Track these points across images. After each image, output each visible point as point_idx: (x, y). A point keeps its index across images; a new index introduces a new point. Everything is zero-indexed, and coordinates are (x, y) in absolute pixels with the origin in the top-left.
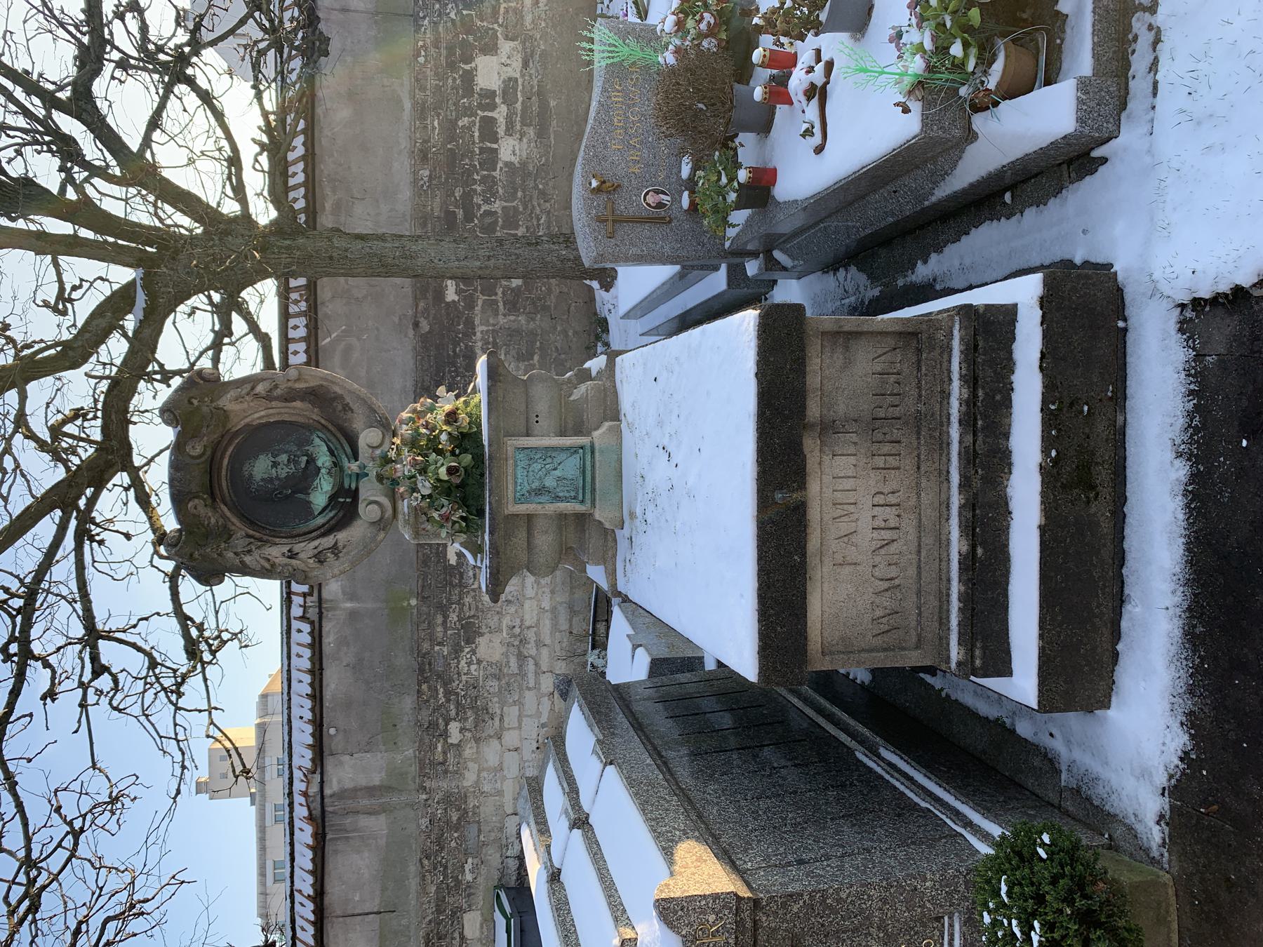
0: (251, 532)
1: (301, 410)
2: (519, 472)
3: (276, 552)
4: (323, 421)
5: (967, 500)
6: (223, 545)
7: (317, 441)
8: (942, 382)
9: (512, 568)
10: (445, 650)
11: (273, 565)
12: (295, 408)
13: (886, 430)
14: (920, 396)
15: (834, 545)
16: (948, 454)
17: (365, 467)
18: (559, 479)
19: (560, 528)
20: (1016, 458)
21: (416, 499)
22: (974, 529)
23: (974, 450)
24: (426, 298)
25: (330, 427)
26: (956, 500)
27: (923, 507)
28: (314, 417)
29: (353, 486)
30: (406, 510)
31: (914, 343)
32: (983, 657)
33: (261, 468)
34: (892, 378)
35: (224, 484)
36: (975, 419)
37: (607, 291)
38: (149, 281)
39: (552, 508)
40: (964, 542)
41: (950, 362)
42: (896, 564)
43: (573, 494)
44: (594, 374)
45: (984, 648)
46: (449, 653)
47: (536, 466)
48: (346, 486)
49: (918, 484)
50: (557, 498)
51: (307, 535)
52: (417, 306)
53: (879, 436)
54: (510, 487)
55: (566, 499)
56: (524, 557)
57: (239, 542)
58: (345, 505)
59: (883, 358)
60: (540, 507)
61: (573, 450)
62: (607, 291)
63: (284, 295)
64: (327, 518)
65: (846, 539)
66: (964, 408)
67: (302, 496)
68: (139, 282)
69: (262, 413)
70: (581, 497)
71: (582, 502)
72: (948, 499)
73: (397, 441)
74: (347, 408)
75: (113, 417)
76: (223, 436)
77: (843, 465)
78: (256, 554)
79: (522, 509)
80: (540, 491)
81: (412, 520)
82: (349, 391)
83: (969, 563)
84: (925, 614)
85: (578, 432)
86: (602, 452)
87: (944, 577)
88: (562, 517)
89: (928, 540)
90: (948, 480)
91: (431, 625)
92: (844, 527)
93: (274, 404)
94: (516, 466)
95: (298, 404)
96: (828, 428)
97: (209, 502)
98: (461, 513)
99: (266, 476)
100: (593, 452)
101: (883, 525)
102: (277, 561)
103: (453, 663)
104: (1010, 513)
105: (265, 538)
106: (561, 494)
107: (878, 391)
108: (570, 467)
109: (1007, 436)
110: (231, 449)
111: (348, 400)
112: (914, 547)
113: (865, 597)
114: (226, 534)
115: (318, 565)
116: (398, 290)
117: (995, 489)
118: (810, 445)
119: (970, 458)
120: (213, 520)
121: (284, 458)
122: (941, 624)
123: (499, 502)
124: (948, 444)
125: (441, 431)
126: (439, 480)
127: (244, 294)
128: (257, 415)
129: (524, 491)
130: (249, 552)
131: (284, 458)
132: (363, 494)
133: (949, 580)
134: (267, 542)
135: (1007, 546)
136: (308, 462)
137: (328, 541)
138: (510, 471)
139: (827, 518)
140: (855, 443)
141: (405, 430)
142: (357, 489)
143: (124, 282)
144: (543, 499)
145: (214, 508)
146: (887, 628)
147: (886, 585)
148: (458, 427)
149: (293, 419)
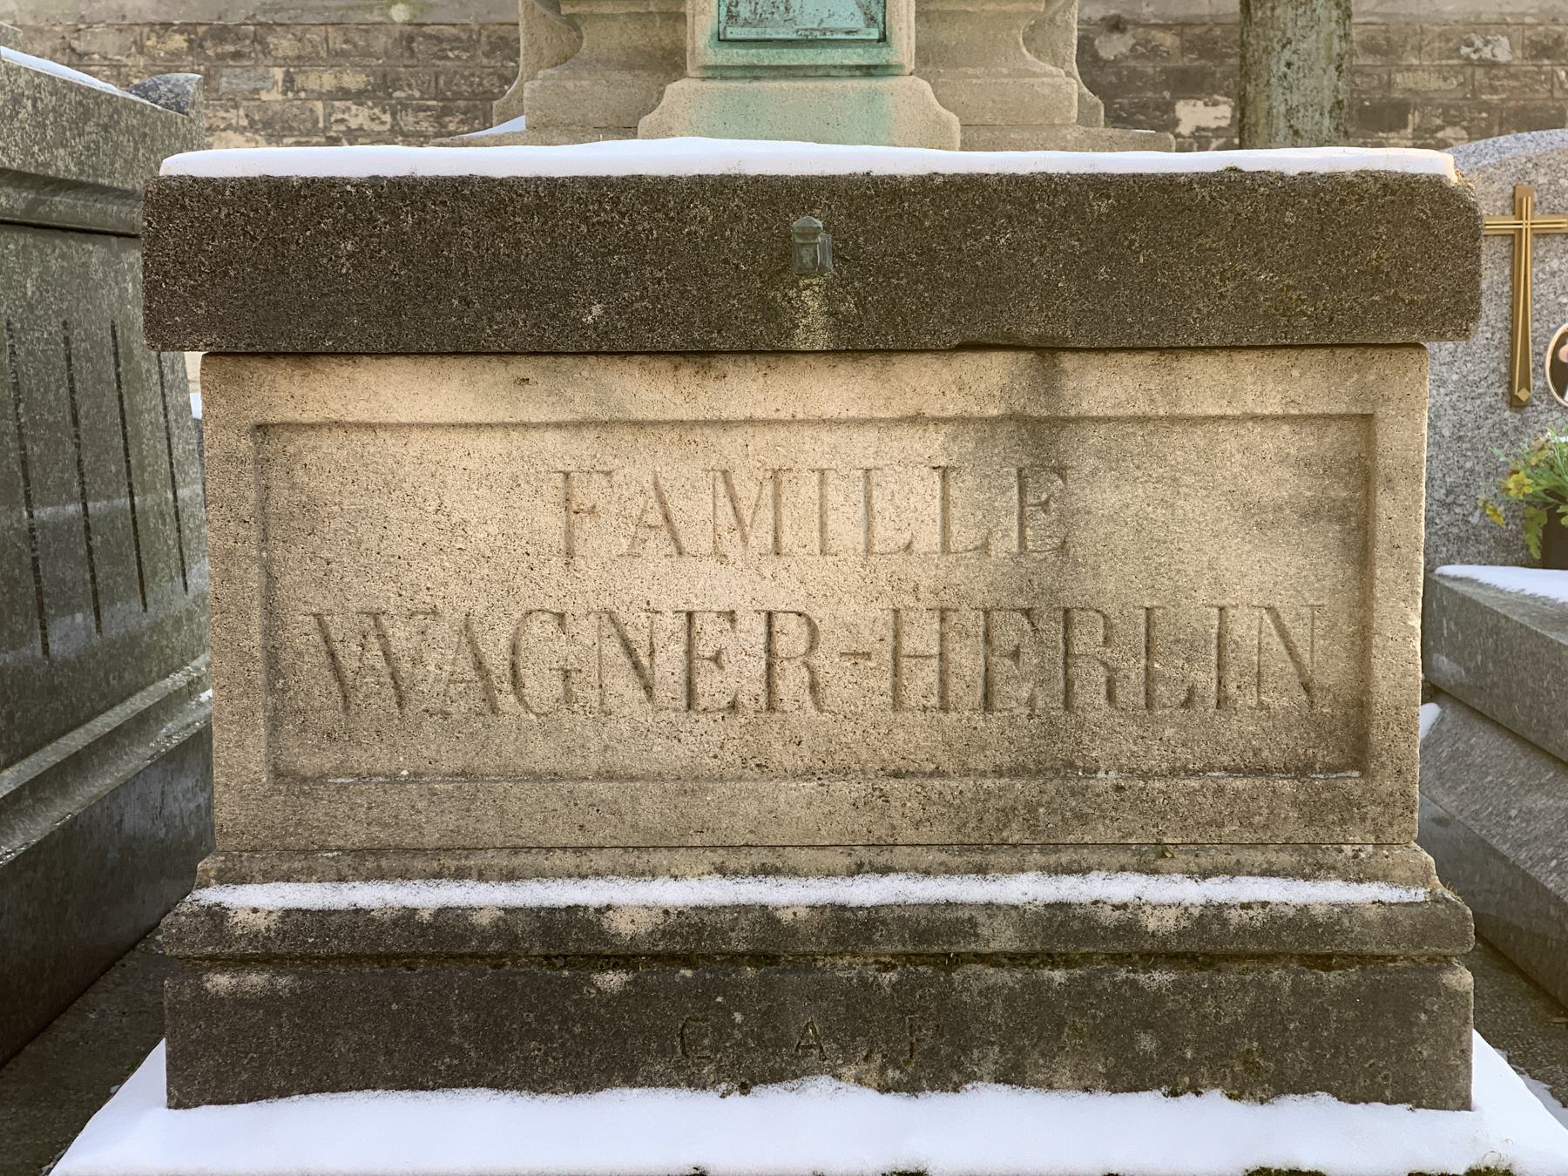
5: (791, 931)
8: (1198, 848)
10: (272, 96)
13: (1030, 659)
14: (1146, 776)
15: (638, 467)
16: (950, 871)
20: (934, 1107)
22: (687, 960)
23: (959, 960)
24: (1184, 51)
26: (790, 895)
27: (766, 787)
31: (1322, 756)
32: (239, 1001)
34: (1205, 678)
36: (1068, 963)
40: (645, 924)
41: (1268, 872)
42: (568, 697)
45: (269, 1002)
46: (263, 106)
49: (844, 772)
52: (1165, 27)
53: (1007, 636)
59: (1276, 643)
65: (655, 517)
66: (1108, 917)
70: (734, 32)
72: (794, 872)
77: (912, 504)
83: (573, 941)
84: (393, 797)
86: (872, 98)
87: (517, 861)
89: (651, 808)
90: (857, 870)
91: (336, 58)
92: (698, 509)
96: (1038, 444)
100: (868, 71)
101: (705, 649)
103: (238, 117)
104: (745, 1089)
107: (1162, 629)
109: (1012, 1075)
112: (622, 759)
113: (455, 588)
117: (830, 1034)
118: (989, 381)
119: (936, 940)
122: (360, 853)
124: (981, 870)
133: (511, 876)
135: (630, 1081)
139: (730, 445)
140: (984, 548)
146: (349, 664)
147: (497, 661)
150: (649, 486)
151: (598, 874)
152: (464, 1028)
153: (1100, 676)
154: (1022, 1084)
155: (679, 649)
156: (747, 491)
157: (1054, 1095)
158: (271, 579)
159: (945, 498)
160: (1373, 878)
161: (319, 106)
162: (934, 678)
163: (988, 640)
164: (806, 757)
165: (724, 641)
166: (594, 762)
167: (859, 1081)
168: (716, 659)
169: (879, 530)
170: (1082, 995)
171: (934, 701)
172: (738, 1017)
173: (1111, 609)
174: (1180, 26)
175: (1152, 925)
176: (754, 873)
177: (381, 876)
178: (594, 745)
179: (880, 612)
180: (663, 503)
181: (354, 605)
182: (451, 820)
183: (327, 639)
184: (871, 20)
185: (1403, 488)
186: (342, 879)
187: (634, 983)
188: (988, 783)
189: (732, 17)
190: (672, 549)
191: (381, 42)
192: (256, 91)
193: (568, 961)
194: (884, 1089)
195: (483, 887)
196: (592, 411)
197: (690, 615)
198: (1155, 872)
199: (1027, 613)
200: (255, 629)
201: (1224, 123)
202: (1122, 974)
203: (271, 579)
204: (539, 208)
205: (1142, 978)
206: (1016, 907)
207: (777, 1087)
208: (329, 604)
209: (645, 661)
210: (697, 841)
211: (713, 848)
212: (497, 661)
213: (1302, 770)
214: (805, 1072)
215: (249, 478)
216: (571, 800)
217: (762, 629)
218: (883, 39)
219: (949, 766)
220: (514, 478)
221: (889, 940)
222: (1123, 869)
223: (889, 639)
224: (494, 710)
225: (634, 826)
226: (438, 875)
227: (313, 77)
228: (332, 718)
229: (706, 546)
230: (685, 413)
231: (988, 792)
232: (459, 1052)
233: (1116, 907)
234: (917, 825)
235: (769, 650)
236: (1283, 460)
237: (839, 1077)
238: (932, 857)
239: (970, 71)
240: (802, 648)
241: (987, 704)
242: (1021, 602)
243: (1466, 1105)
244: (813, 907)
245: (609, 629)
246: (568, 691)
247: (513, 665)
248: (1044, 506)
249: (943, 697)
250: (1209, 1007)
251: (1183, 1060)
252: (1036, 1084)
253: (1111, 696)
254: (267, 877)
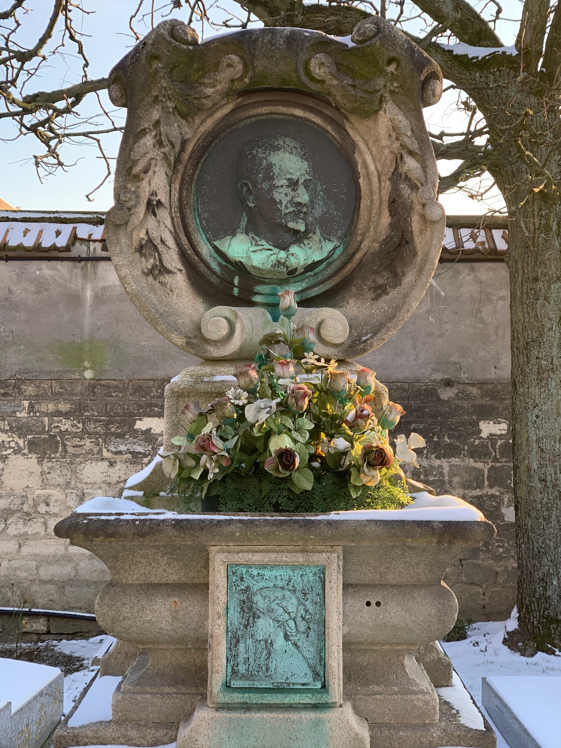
0: (190, 147)
1: (376, 224)
2: (282, 573)
3: (157, 182)
4: (358, 256)
6: (170, 104)
7: (328, 247)
9: (115, 558)
11: (137, 178)
12: (379, 215)
17: (289, 316)
18: (269, 644)
19: (182, 641)
21: (238, 398)
24: (483, 396)
25: (350, 267)
28: (365, 244)
29: (257, 299)
30: (218, 378)
33: (289, 163)
35: (260, 110)
37: (505, 642)
38: (501, 61)
39: (218, 630)
43: (242, 669)
44: (445, 693)
46: (18, 420)
47: (292, 604)
48: (258, 288)
50: (234, 640)
51: (183, 229)
52: (473, 385)
54: (257, 558)
55: (232, 657)
56: (134, 576)
57: (175, 129)
58: (228, 286)
60: (221, 609)
61: (320, 671)
62: (505, 642)
63: (489, 224)
64: (209, 260)
67: (243, 224)
68: (501, 50)
69: (372, 167)
70: (236, 684)
71: (227, 686)
73: (332, 367)
74: (380, 291)
75: (332, 18)
76: (337, 108)
78: (156, 153)
79: (218, 577)
80: (249, 611)
81: (202, 387)
82: (406, 296)
85: (351, 674)
86: (317, 724)
88: (202, 644)
91: (56, 397)
93: (387, 185)
94: (294, 567)
95: (386, 220)
97: (238, 86)
98: (214, 471)
99: (276, 170)
100: (315, 707)
102: (145, 183)
105: (181, 168)
106: (241, 647)
108: (290, 665)
110: (317, 120)
111: (393, 293)
114: (188, 111)
115: (136, 243)
116: (498, 363)
120: (209, 91)
121: (303, 197)
123: (231, 537)
125: (350, 440)
126: (268, 435)
127: (487, 175)
128: (369, 159)
129: (249, 582)
130: (160, 143)
131: (303, 197)
132: (244, 312)
134: (175, 170)
136: (296, 232)
137: (172, 259)
138: (286, 558)
141: (349, 379)
142: (252, 304)
143: (498, 33)
144: (235, 615)
145: (228, 94)
148: (359, 469)
149: (363, 212)
161: (46, 419)
174: (481, 384)
184: (316, 675)
189: (234, 672)
191: (79, 388)
192: (14, 412)
201: (504, 432)
218: (324, 686)
227: (43, 405)
239: (376, 688)
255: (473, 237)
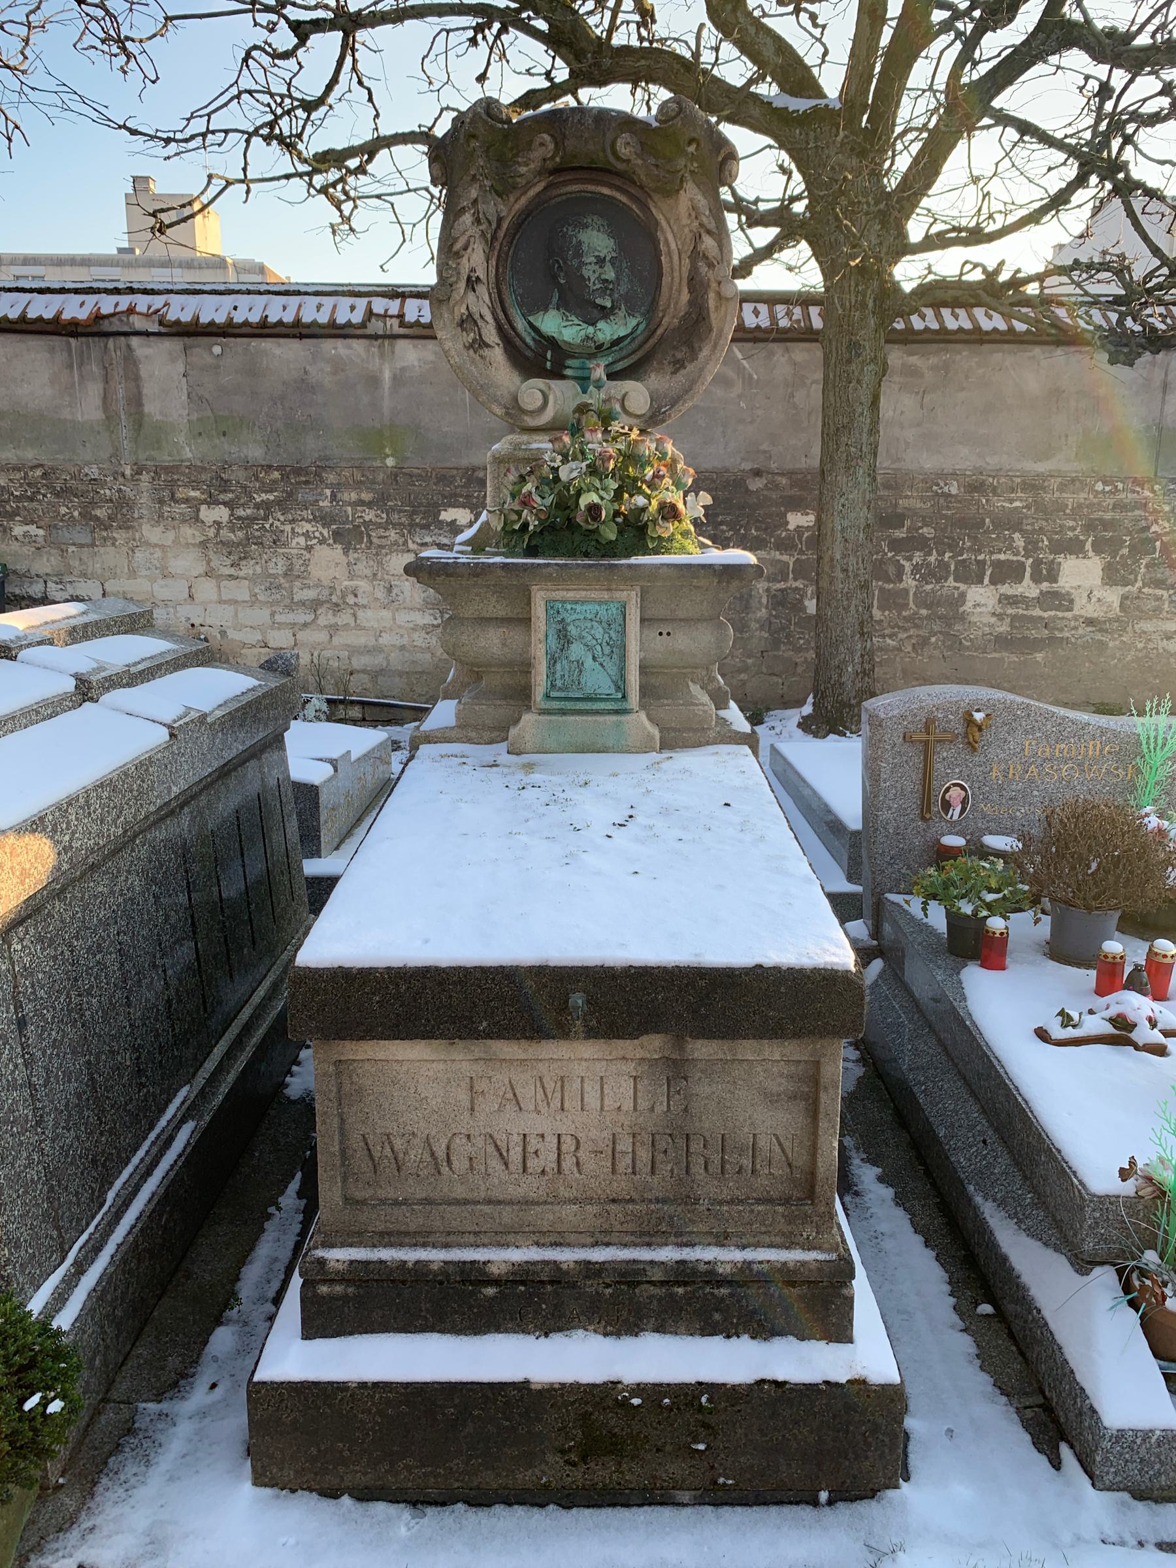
0: (505, 226)
1: (676, 299)
2: (592, 608)
3: (476, 259)
4: (659, 332)
5: (567, 1273)
6: (487, 183)
7: (633, 322)
8: (741, 1235)
9: (454, 595)
10: (325, 504)
11: (458, 255)
12: (679, 291)
13: (672, 1154)
14: (721, 1203)
15: (501, 1077)
16: (635, 1245)
17: (599, 388)
18: (580, 664)
19: (511, 663)
20: (627, 1344)
21: (553, 460)
22: (523, 1283)
23: (639, 1283)
24: (792, 486)
25: (652, 342)
26: (567, 1256)
27: (557, 1208)
28: (665, 321)
29: (568, 372)
30: (535, 446)
31: (796, 1194)
32: (332, 1298)
33: (597, 241)
34: (746, 1162)
35: (570, 188)
36: (685, 1284)
37: (799, 725)
38: (823, 116)
39: (540, 654)
40: (504, 1269)
41: (771, 1246)
42: (472, 1168)
43: (559, 683)
44: (722, 713)
45: (345, 1298)
46: (320, 509)
47: (599, 632)
48: (569, 362)
49: (589, 1200)
50: (553, 661)
51: (500, 304)
52: (782, 474)
53: (662, 1145)
54: (571, 595)
55: (551, 673)
56: (469, 611)
57: (492, 207)
58: (540, 359)
59: (777, 1149)
60: (541, 636)
61: (621, 685)
62: (799, 725)
63: (804, 300)
64: (524, 335)
65: (510, 1095)
66: (702, 1268)
67: (555, 300)
68: (823, 102)
69: (673, 246)
70: (554, 694)
71: (547, 696)
72: (569, 1245)
73: (635, 434)
74: (678, 365)
75: (643, 62)
76: (641, 187)
77: (621, 1092)
78: (474, 231)
79: (539, 611)
80: (564, 638)
81: (520, 454)
82: (702, 370)
83: (474, 1275)
84: (396, 1211)
85: (646, 691)
86: (618, 725)
87: (449, 1239)
88: (526, 667)
89: (507, 1215)
90: (595, 1244)
91: (358, 485)
92: (528, 1093)
93: (686, 262)
94: (600, 603)
95: (685, 297)
96: (676, 1071)
97: (550, 165)
98: (533, 524)
99: (585, 247)
100: (617, 712)
101: (531, 1149)
102: (465, 260)
103: (307, 514)
104: (546, 1335)
105: (497, 245)
106: (558, 666)
107: (729, 1142)
108: (597, 680)
109: (660, 1329)
110: (624, 199)
111: (690, 367)
112: (497, 1194)
113: (422, 1124)
114: (503, 190)
115: (457, 318)
116: (805, 450)
117: (583, 1313)
118: (653, 1045)
119: (629, 1276)
120: (523, 170)
121: (610, 274)
122: (382, 1234)
123: (549, 578)
124: (649, 1245)
125: (648, 497)
126: (579, 493)
127: (804, 245)
128: (670, 237)
129: (564, 614)
130: (478, 221)
131: (610, 274)
132: (556, 385)
133: (446, 1246)
134: (492, 247)
135: (498, 1330)
136: (603, 308)
137: (490, 334)
138: (594, 595)
139: (542, 1068)
140: (652, 1109)
141: (648, 447)
142: (563, 377)
143: (821, 81)
144: (553, 642)
145: (540, 173)
146: (376, 1155)
147: (441, 1154)
148: (655, 522)
149: (665, 289)
150: (507, 1083)
151: (484, 1245)
152: (427, 1310)
153: (701, 1161)
154: (664, 1333)
155: (519, 1149)
156: (550, 1086)
157: (677, 1338)
158: (343, 1121)
159: (635, 1087)
160: (814, 1248)
161: (349, 509)
162: (630, 1162)
163: (653, 1145)
164: (573, 1193)
165: (539, 1146)
166: (483, 1195)
167: (595, 1331)
168: (536, 1153)
169: (606, 1102)
170: (691, 1298)
171: (630, 1170)
172: (544, 1306)
173: (707, 1135)
174: (790, 474)
175: (721, 1271)
176: (551, 1245)
177: (391, 1245)
178: (483, 1188)
179: (607, 1134)
180: (513, 1089)
181: (378, 1131)
182: (421, 1221)
183: (367, 1144)
184: (618, 688)
185: (831, 1091)
186: (374, 1246)
187: (499, 1292)
188: (652, 1207)
189: (553, 686)
190: (517, 1108)
191: (381, 477)
192: (317, 501)
193: (471, 1283)
194: (606, 1335)
195: (434, 1251)
196: (483, 1055)
197: (524, 1135)
198: (723, 1245)
199: (670, 1135)
200: (336, 1143)
201: (811, 524)
202: (708, 1290)
203: (343, 1121)
204: (460, 982)
205: (716, 1291)
206: (663, 1263)
207: (560, 1334)
208: (368, 1130)
209: (505, 1154)
210: (527, 1229)
211: (534, 1233)
212: (441, 1154)
213: (786, 1201)
214: (572, 1328)
215: (333, 1082)
216: (472, 1213)
217: (556, 1141)
218: (624, 697)
219: (635, 1196)
220: (448, 1079)
221: (609, 1276)
222: (709, 1244)
223: (611, 1146)
224: (439, 1173)
225: (500, 1224)
226: (415, 1245)
227: (346, 494)
228: (369, 1175)
229: (532, 1107)
230: (522, 1056)
231: (653, 1211)
232: (426, 1318)
233: (706, 1263)
234: (622, 1224)
235: (559, 1149)
236: (781, 1075)
237: (587, 1330)
238: (628, 1238)
239: (666, 702)
240: (573, 1148)
241: (653, 1172)
242: (668, 1131)
243: (851, 1341)
244: (576, 1262)
245: (489, 1141)
246: (471, 1165)
247: (448, 1154)
248: (678, 1093)
249: (634, 1168)
250: (744, 1302)
251: (732, 1323)
252: (671, 1333)
253: (706, 1168)
254: (343, 1245)
255: (756, 313)
